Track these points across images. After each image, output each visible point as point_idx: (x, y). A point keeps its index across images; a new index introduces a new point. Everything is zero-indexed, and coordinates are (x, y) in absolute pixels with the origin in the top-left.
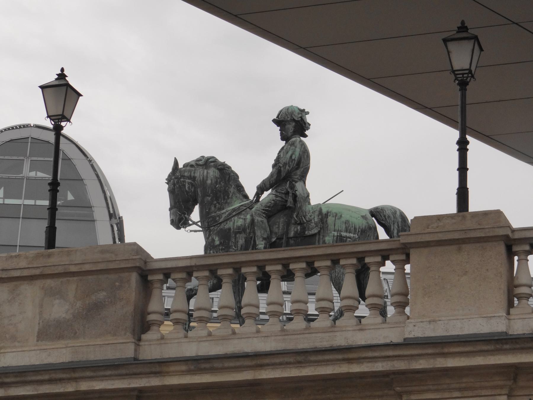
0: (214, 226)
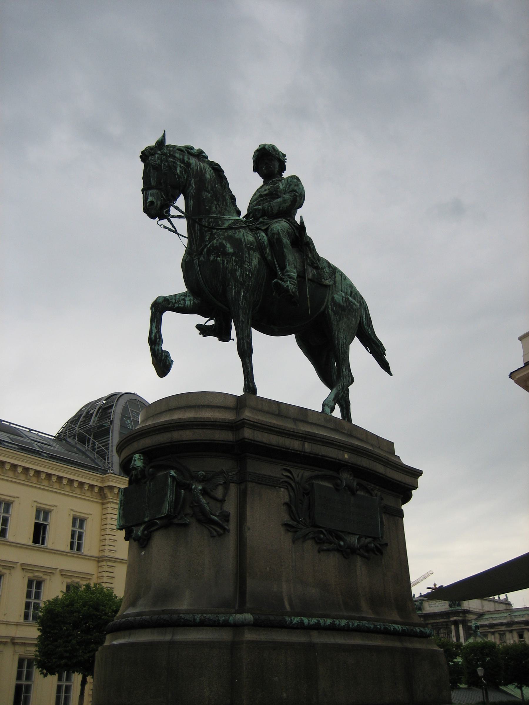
0: (218, 229)
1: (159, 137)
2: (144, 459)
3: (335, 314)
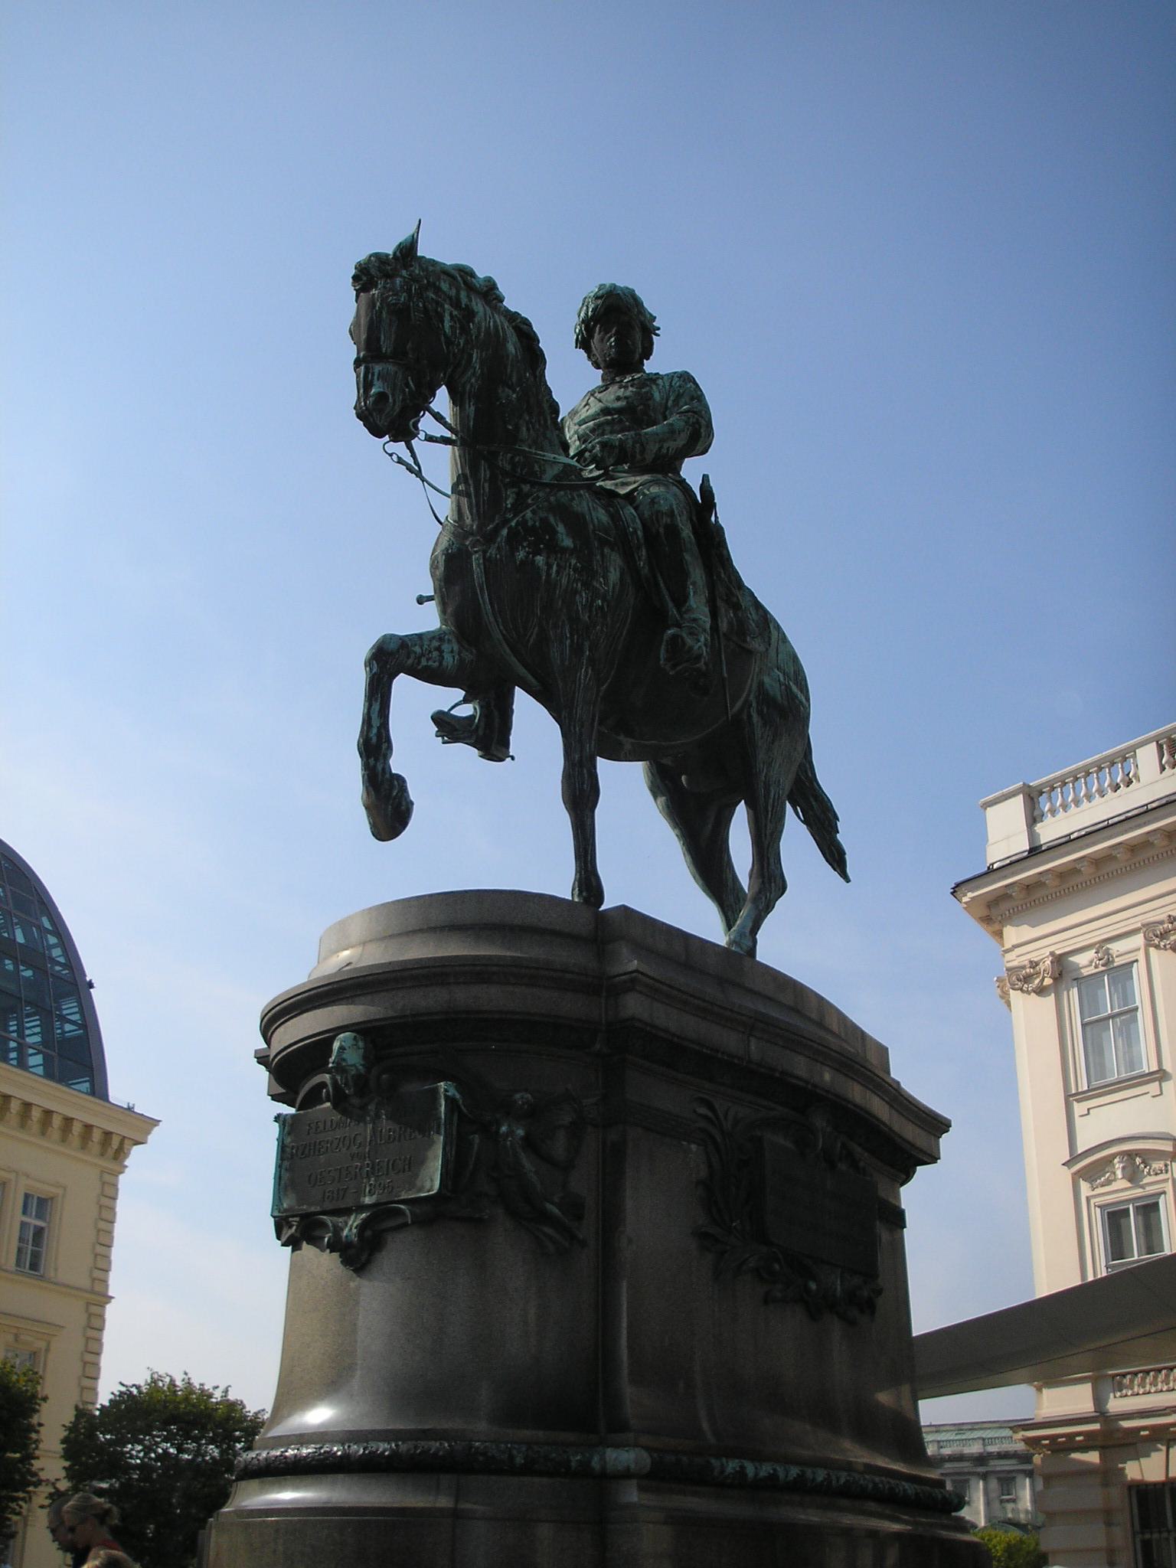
0: (533, 484)
1: (402, 236)
2: (365, 1049)
3: (765, 725)
